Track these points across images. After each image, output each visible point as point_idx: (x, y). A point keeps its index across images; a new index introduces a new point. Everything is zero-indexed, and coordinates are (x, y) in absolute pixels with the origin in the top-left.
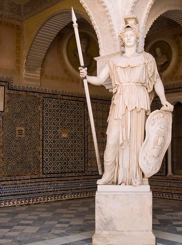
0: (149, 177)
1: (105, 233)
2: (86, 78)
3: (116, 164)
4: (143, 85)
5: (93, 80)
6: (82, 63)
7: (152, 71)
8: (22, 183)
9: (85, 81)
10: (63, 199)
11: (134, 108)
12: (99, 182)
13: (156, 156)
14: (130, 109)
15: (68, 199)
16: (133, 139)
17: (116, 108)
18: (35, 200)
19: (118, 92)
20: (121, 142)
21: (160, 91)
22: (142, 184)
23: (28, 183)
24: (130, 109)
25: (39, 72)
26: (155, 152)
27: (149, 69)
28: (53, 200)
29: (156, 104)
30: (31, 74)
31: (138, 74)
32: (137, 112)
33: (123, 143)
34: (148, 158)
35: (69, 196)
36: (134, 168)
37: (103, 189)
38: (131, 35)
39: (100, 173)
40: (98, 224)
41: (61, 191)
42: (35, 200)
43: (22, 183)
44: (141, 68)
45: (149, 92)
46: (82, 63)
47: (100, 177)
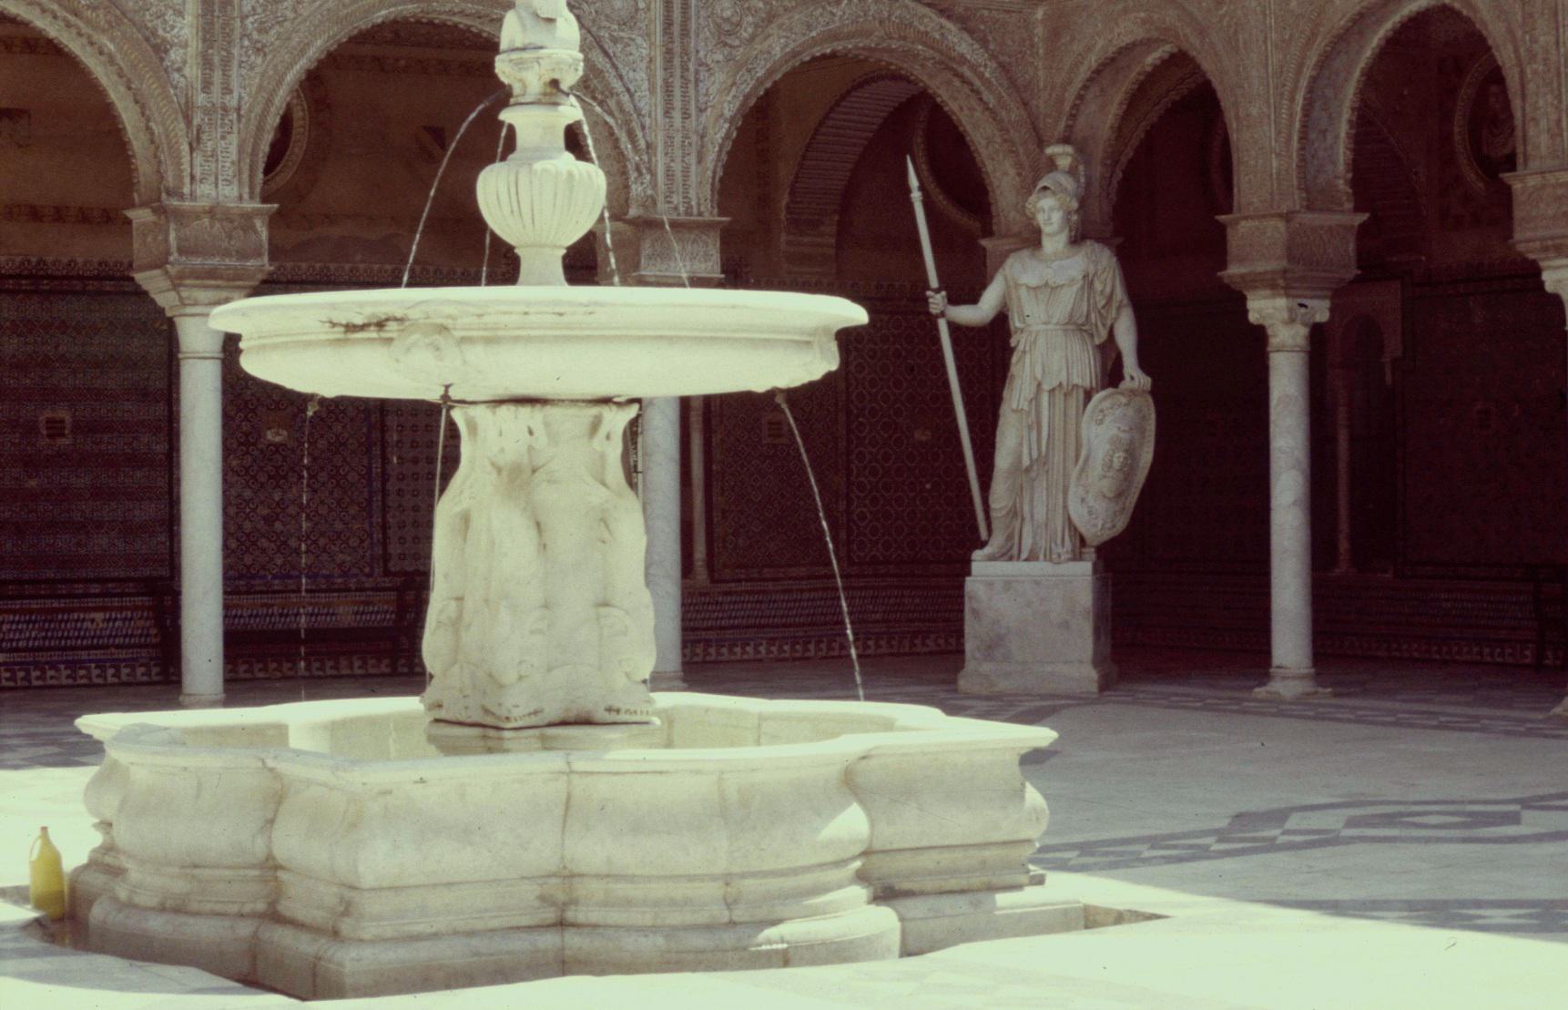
0: (1096, 543)
1: (986, 667)
2: (943, 314)
3: (1014, 513)
4: (1080, 329)
5: (967, 314)
6: (934, 281)
7: (1108, 290)
8: (785, 591)
9: (943, 325)
10: (919, 649)
11: (1055, 383)
12: (977, 554)
13: (1110, 495)
14: (1046, 387)
15: (935, 648)
16: (1057, 458)
17: (1017, 383)
18: (823, 646)
19: (1021, 347)
20: (1026, 462)
21: (1127, 340)
22: (1077, 557)
23: (802, 591)
24: (1046, 387)
25: (834, 229)
26: (1107, 486)
27: (1098, 286)
28: (884, 650)
29: (1112, 375)
30: (806, 240)
31: (1067, 299)
32: (1065, 395)
33: (1031, 466)
34: (1090, 500)
35: (941, 641)
36: (1059, 522)
37: (981, 565)
38: (1052, 209)
39: (984, 534)
40: (969, 646)
41: (911, 621)
42: (823, 646)
43: (785, 591)
44: (1075, 288)
45: (1097, 341)
46: (934, 281)
47: (983, 545)
